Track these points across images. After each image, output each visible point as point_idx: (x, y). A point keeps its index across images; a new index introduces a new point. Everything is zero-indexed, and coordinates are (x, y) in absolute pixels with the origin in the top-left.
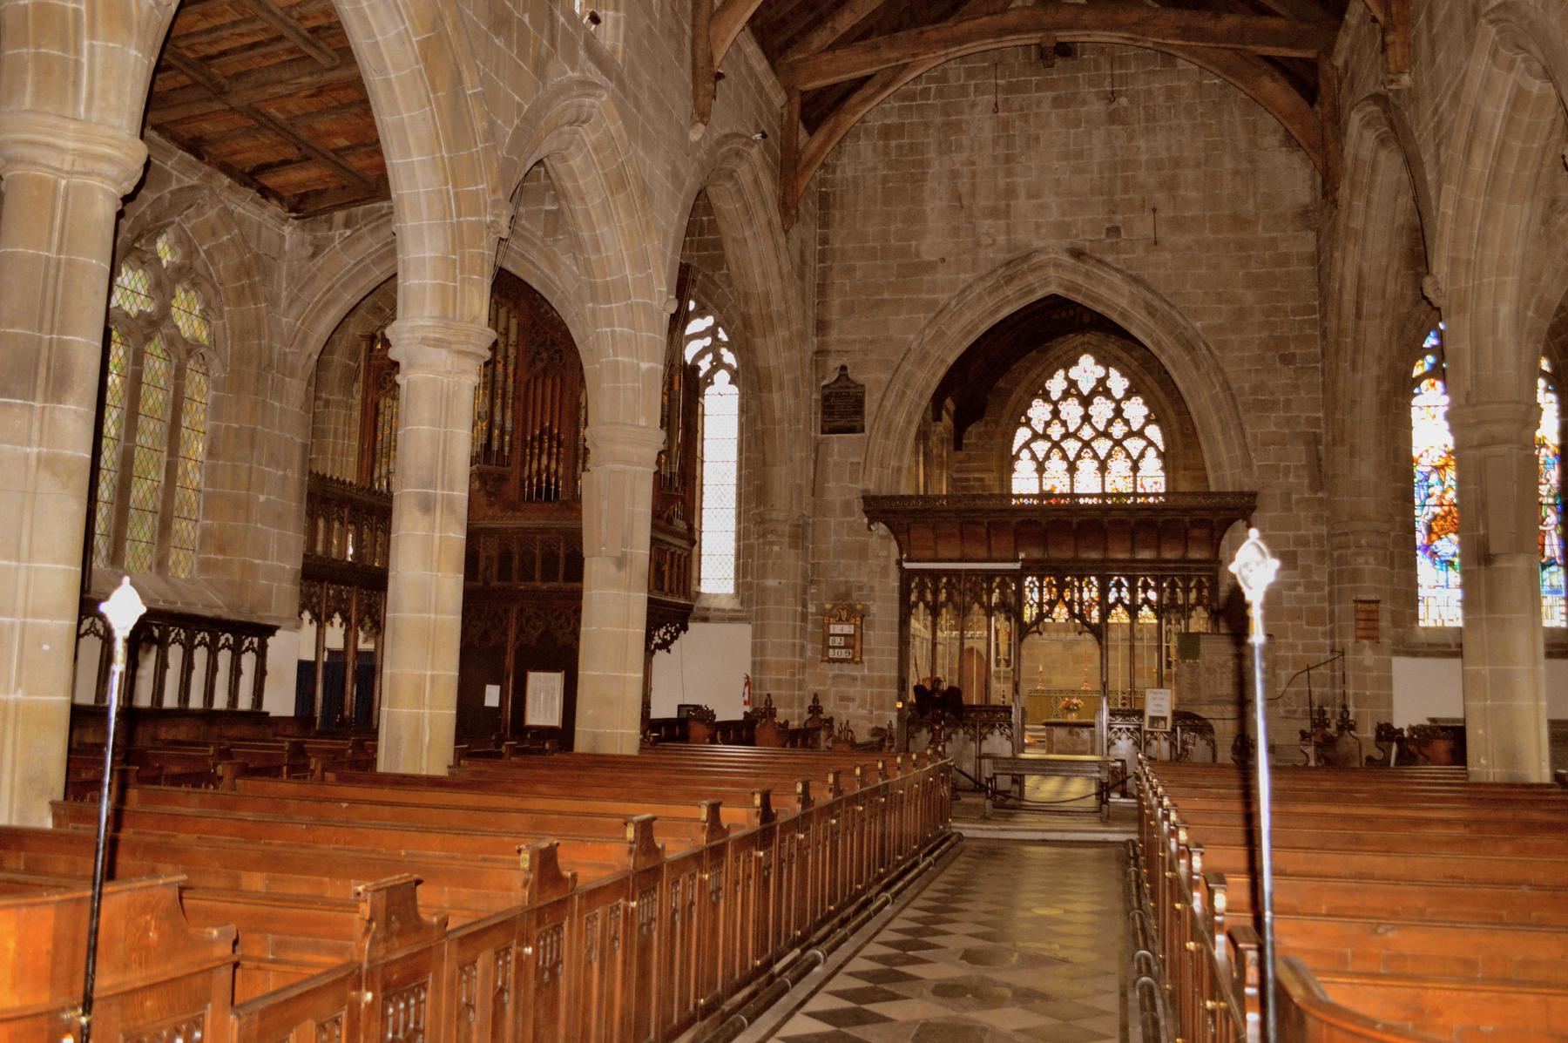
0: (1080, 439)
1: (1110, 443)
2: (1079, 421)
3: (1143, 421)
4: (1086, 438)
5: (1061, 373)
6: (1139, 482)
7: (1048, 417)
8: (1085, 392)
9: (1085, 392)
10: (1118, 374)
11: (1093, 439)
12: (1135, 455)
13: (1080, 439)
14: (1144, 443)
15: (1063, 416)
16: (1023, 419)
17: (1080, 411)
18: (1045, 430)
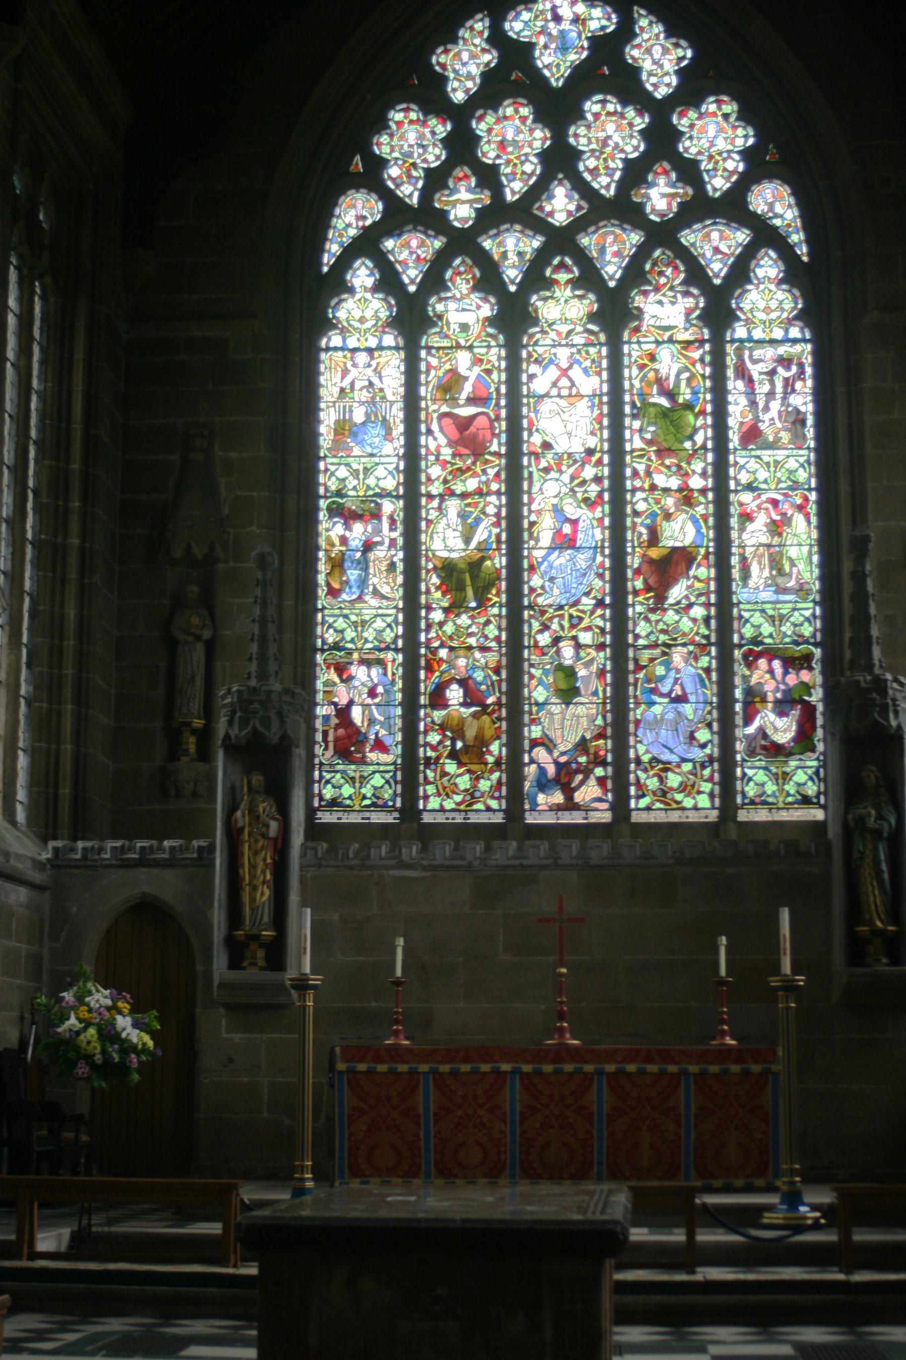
0: (539, 225)
1: (635, 238)
2: (533, 167)
3: (736, 165)
4: (560, 219)
5: (481, 24)
6: (731, 360)
7: (435, 156)
8: (557, 83)
9: (557, 83)
10: (658, 28)
11: (579, 224)
12: (717, 269)
13: (539, 225)
14: (742, 236)
15: (488, 153)
16: (358, 163)
17: (540, 138)
18: (427, 194)
